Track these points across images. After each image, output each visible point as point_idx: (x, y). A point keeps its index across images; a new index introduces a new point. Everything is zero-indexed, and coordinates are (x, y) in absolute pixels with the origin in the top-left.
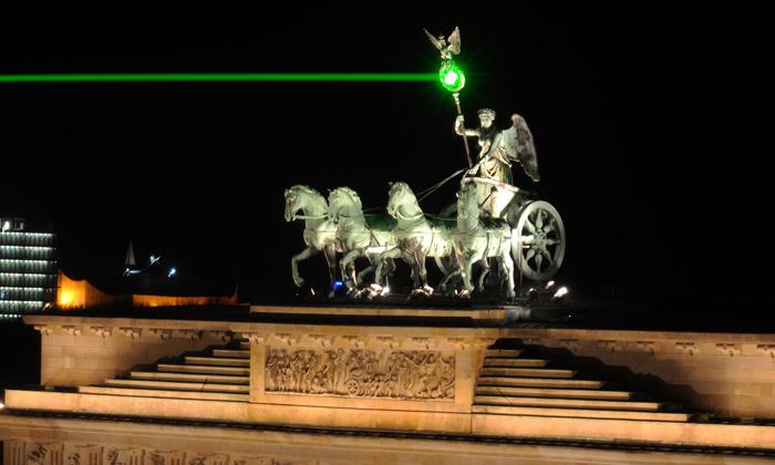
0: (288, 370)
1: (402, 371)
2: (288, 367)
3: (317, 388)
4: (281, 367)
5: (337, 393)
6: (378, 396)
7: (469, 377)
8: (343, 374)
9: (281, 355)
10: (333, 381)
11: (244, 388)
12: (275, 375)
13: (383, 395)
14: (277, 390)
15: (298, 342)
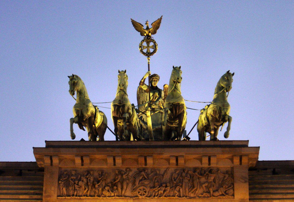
0: (80, 183)
1: (186, 181)
2: (80, 180)
3: (107, 194)
4: (74, 180)
5: (126, 196)
6: (165, 196)
7: (245, 182)
8: (130, 185)
9: (73, 173)
10: (122, 189)
11: (39, 197)
12: (67, 186)
13: (170, 196)
14: (69, 196)
15: (90, 164)
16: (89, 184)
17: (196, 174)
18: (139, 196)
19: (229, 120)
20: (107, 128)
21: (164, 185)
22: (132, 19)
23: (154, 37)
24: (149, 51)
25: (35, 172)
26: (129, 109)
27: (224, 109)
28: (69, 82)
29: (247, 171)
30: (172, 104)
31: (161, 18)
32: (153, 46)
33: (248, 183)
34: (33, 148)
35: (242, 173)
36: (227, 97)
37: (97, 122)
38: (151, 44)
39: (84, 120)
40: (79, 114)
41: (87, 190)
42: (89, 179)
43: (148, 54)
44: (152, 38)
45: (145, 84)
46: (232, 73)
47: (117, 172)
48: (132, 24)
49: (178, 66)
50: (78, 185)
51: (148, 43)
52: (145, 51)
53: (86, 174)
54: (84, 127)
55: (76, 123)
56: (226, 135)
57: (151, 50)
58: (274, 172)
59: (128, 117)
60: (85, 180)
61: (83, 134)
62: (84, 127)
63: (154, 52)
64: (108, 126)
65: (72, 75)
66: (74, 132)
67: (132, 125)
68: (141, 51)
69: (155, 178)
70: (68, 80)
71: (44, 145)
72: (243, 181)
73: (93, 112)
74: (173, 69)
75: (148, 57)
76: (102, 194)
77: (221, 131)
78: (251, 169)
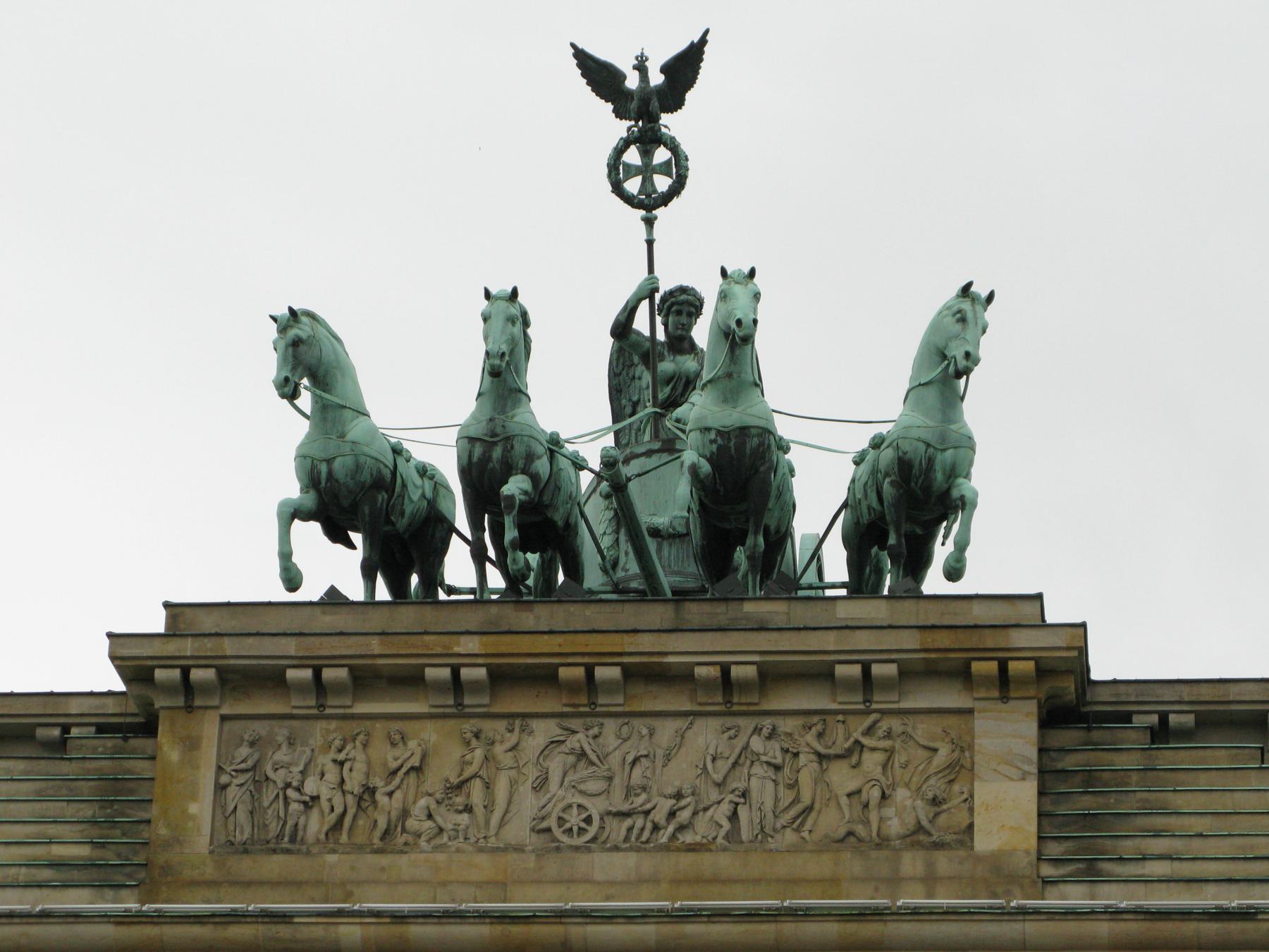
7: (1023, 779)
16: (347, 787)
17: (810, 737)
18: (565, 839)
20: (454, 536)
21: (670, 790)
22: (573, 45)
23: (670, 122)
24: (653, 184)
25: (125, 739)
26: (530, 457)
27: (944, 450)
28: (275, 343)
30: (719, 432)
31: (703, 41)
32: (668, 163)
33: (1035, 783)
34: (110, 635)
35: (1009, 733)
36: (962, 399)
37: (402, 514)
38: (661, 155)
39: (346, 503)
40: (320, 483)
41: (339, 810)
42: (347, 766)
43: (649, 203)
44: (663, 130)
45: (639, 333)
46: (984, 294)
47: (468, 735)
48: (580, 65)
49: (746, 270)
50: (298, 790)
51: (646, 154)
53: (337, 743)
54: (350, 533)
55: (307, 516)
56: (954, 573)
57: (662, 183)
58: (1161, 733)
59: (526, 493)
60: (332, 775)
61: (335, 567)
62: (350, 533)
63: (677, 188)
64: (457, 525)
65: (287, 311)
66: (294, 559)
67: (553, 524)
68: (618, 189)
69: (630, 758)
71: (156, 623)
72: (1014, 773)
73: (382, 466)
74: (720, 280)
75: (649, 207)
76: (404, 830)
77: (943, 544)
78: (1055, 717)
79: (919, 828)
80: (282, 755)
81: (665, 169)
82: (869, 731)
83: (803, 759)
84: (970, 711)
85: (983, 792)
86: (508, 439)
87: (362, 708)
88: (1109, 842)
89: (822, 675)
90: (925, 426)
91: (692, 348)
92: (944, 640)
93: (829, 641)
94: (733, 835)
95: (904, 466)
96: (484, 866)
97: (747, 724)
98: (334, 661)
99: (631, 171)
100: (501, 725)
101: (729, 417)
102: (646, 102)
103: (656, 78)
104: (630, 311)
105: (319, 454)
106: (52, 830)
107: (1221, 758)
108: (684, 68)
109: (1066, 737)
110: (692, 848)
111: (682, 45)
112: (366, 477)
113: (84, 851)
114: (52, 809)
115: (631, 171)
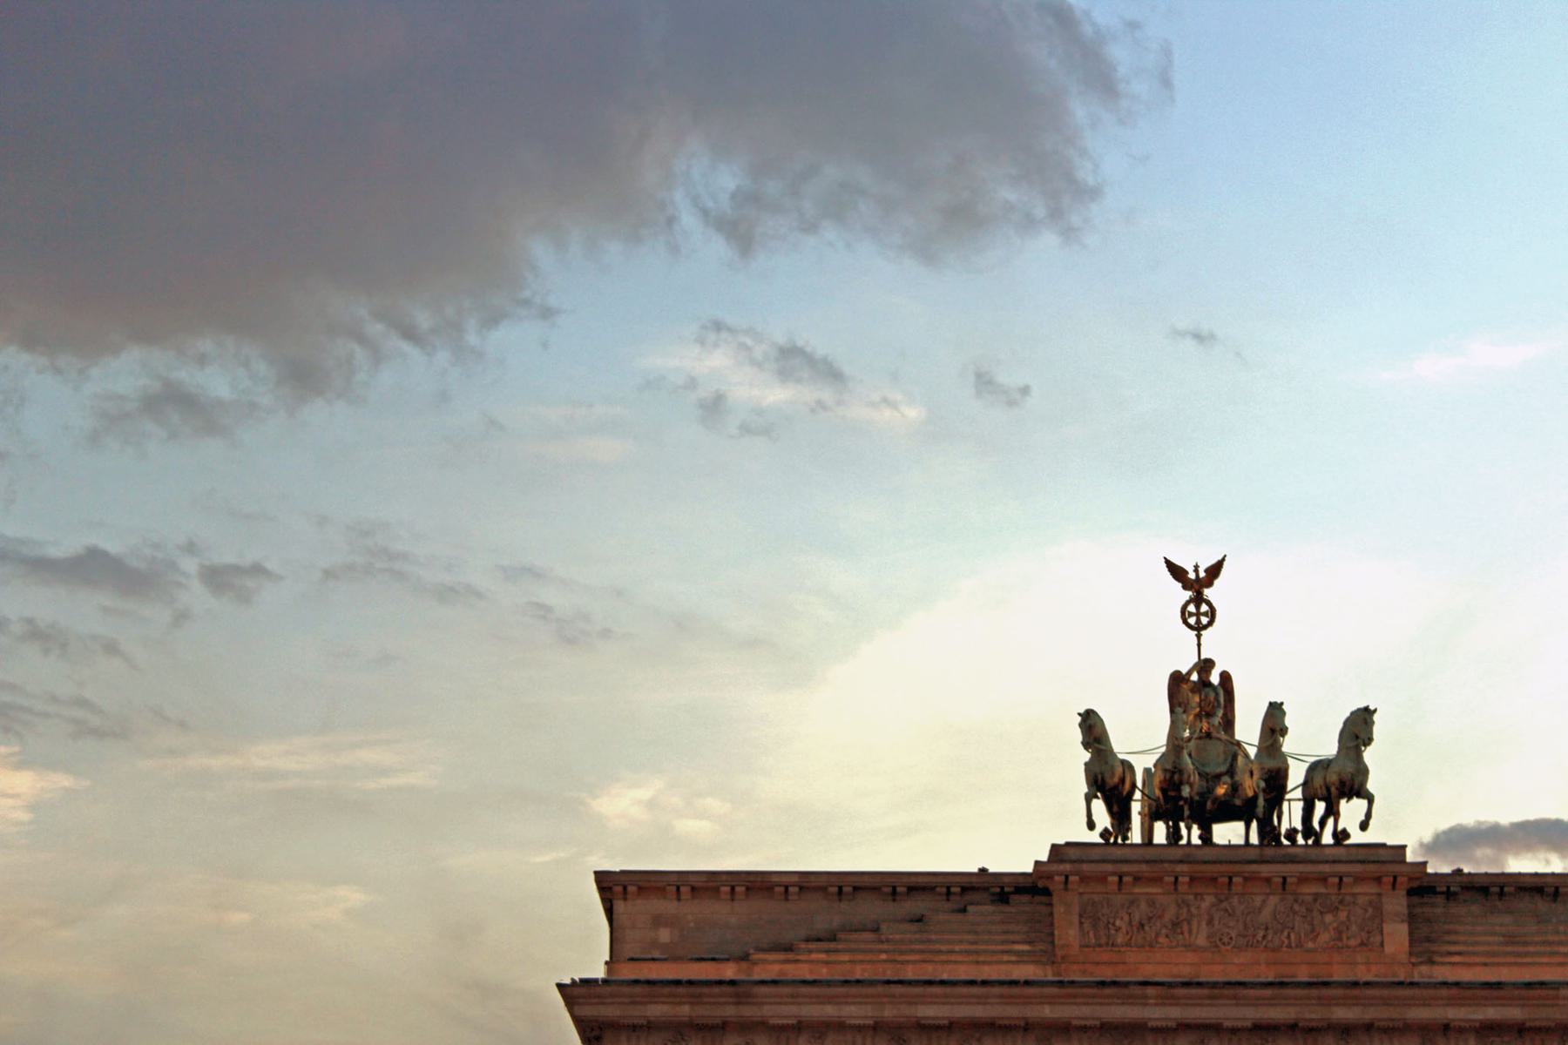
14: (1100, 946)
19: (1370, 799)
23: (1208, 593)
29: (1404, 901)
35: (1396, 903)
38: (1204, 608)
43: (1199, 629)
51: (1198, 607)
52: (1192, 621)
56: (1364, 826)
57: (1204, 620)
58: (1449, 895)
60: (1126, 918)
63: (1210, 623)
68: (1185, 622)
70: (1079, 719)
78: (1411, 892)
79: (1362, 944)
80: (1105, 910)
81: (1206, 614)
82: (1341, 902)
83: (1315, 913)
84: (1380, 895)
85: (1387, 928)
86: (1181, 772)
87: (1137, 890)
88: (1434, 948)
89: (1323, 879)
90: (1350, 768)
91: (1210, 684)
92: (1372, 868)
93: (1327, 868)
94: (1289, 946)
95: (1342, 783)
96: (1191, 957)
97: (1291, 898)
98: (1128, 874)
99: (1191, 614)
100: (1191, 897)
101: (1271, 764)
102: (1197, 585)
103: (1202, 574)
104: (1189, 673)
105: (1097, 770)
106: (1011, 937)
107: (1475, 909)
108: (1215, 571)
109: (1416, 899)
110: (1273, 950)
111: (1213, 561)
112: (1116, 780)
113: (1026, 947)
114: (1012, 927)
115: (1191, 614)
